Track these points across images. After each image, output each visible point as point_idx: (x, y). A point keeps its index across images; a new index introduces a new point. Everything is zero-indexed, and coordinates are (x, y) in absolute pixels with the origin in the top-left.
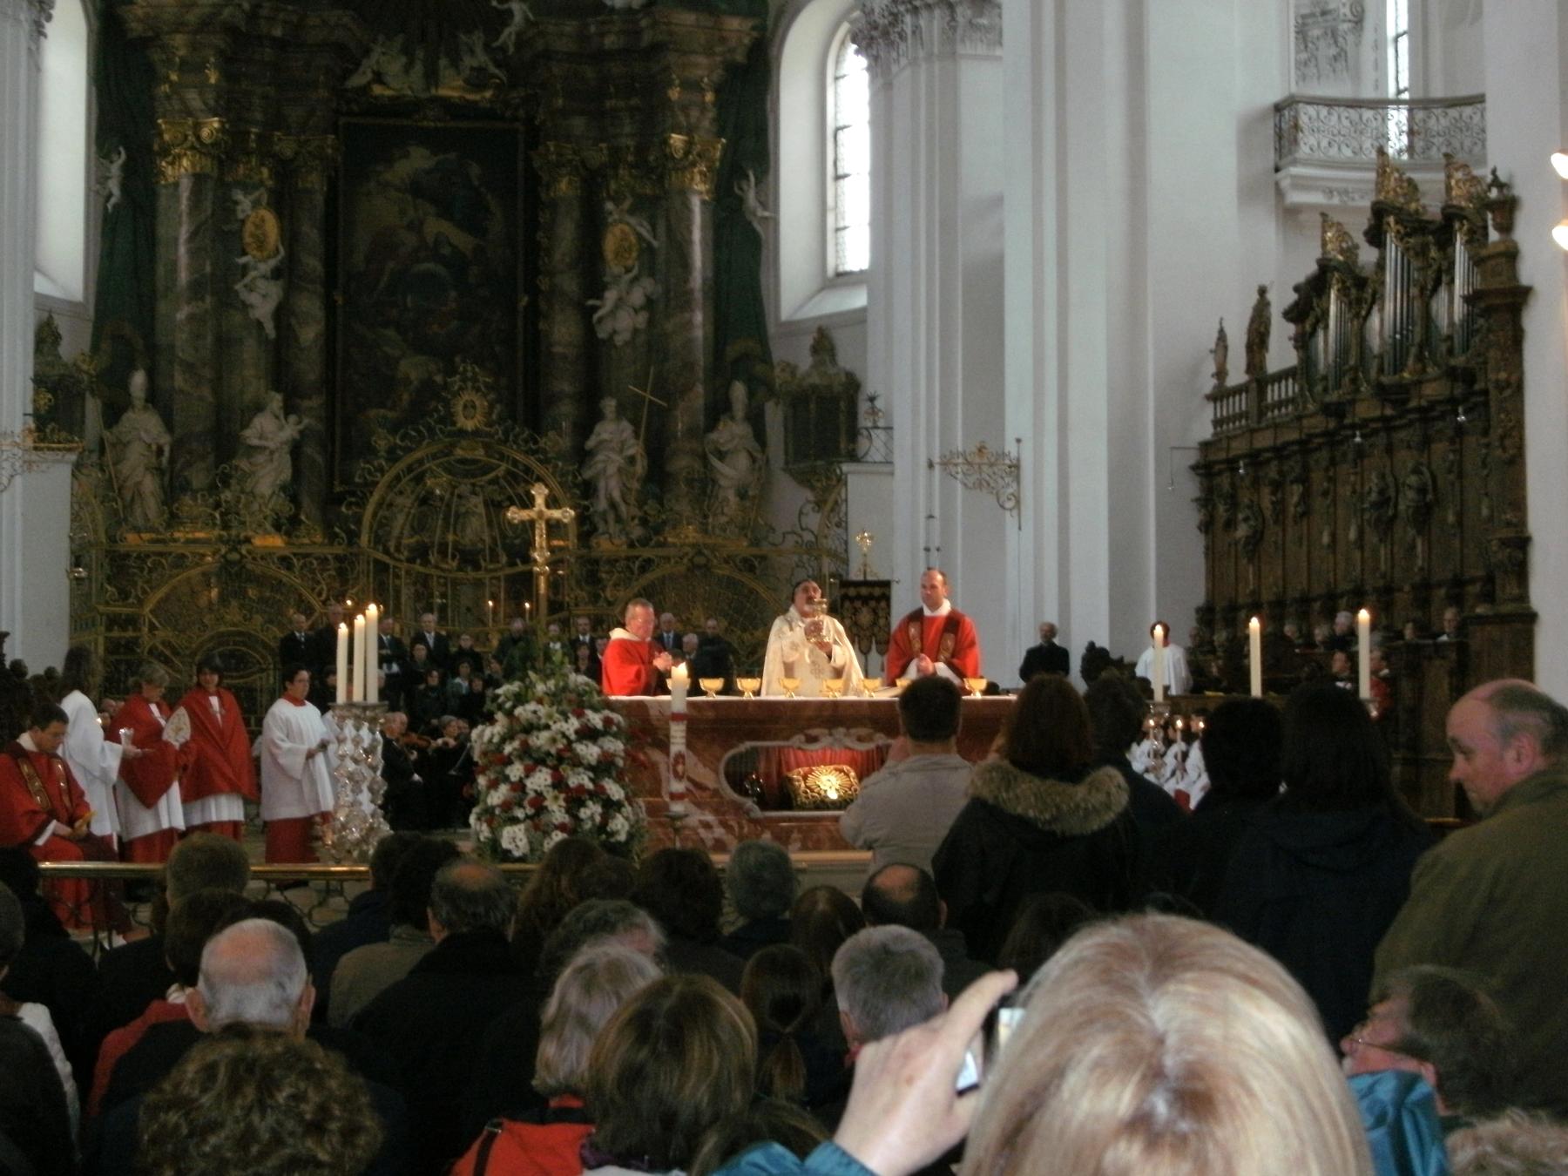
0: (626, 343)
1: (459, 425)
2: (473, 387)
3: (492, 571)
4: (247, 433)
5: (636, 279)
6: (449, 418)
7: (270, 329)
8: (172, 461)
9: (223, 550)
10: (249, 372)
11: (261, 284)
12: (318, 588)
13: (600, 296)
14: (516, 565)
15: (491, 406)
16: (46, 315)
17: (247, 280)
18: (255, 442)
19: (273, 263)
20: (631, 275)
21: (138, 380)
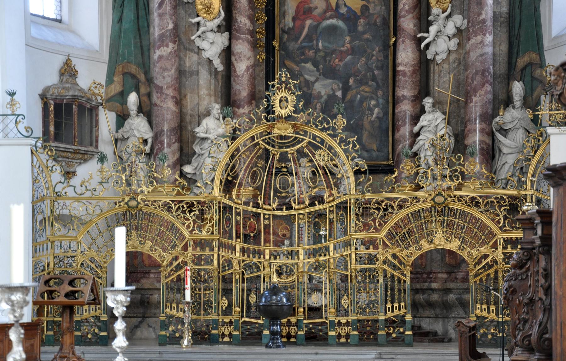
0: (444, 61)
1: (277, 114)
2: (286, 88)
3: (299, 209)
4: (197, 130)
5: (448, 17)
6: (269, 110)
7: (218, 64)
8: (152, 148)
9: (127, 199)
10: (203, 92)
11: (210, 35)
12: (187, 223)
13: (428, 32)
14: (315, 205)
15: (299, 101)
16: (63, 59)
17: (199, 33)
18: (203, 135)
19: (217, 22)
20: (446, 14)
21: (133, 98)
